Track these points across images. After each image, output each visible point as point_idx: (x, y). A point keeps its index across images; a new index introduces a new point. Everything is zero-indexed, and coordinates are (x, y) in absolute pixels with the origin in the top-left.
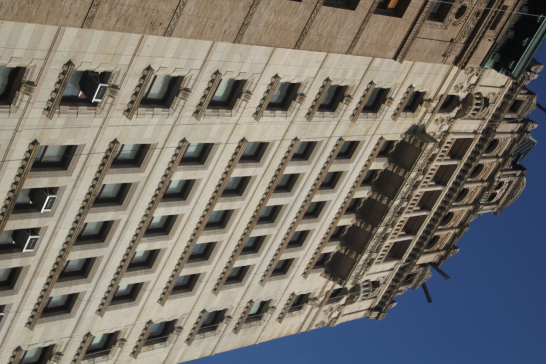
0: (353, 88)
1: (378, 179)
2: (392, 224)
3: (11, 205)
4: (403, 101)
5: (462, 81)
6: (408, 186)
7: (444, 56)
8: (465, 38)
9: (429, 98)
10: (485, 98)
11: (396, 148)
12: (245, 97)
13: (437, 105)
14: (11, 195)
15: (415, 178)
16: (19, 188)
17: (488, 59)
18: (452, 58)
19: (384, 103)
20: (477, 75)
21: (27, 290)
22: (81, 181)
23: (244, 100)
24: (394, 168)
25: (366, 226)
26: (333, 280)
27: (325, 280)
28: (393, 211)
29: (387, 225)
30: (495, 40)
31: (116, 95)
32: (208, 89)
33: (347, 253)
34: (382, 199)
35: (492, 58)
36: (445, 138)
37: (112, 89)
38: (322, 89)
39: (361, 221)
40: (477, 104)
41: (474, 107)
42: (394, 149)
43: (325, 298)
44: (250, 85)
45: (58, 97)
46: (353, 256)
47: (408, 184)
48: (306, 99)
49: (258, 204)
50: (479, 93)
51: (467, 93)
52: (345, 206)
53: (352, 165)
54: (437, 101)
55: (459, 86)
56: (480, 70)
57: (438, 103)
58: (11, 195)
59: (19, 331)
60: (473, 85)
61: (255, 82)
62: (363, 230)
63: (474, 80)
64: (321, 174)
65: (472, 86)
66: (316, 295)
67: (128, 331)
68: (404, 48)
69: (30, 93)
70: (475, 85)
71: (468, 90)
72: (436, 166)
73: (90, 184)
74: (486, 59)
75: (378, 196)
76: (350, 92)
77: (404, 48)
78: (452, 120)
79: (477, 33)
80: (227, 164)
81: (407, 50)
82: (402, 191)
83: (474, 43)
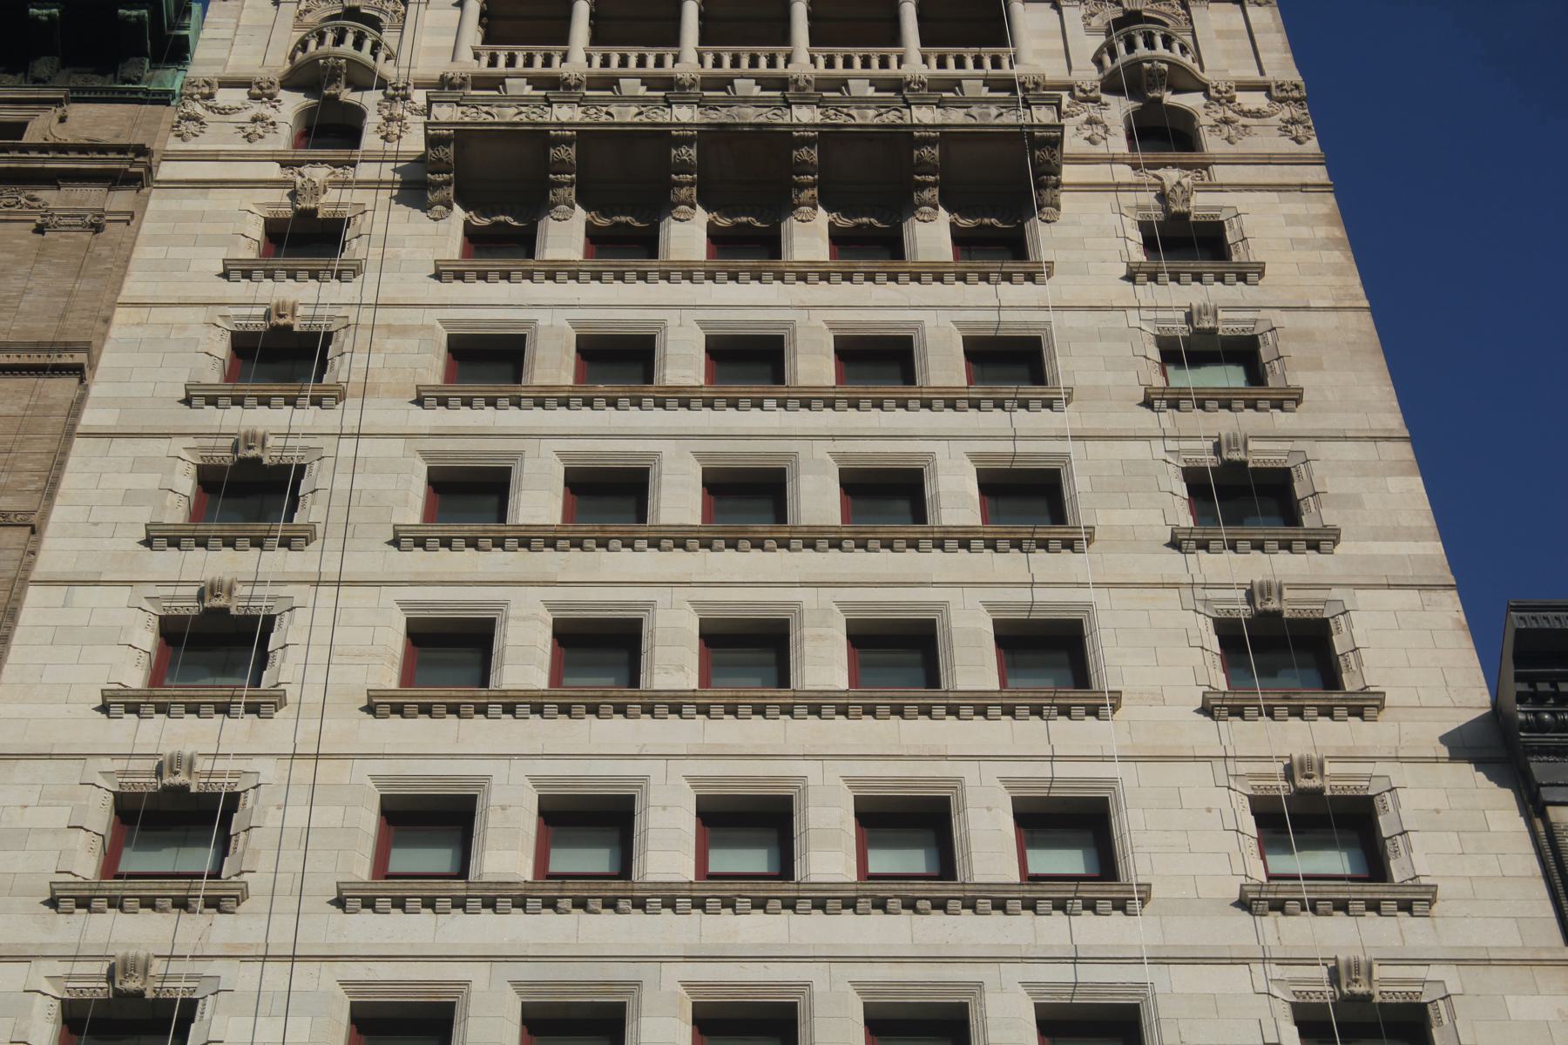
0: (204, 449)
1: (626, 215)
2: (839, 90)
4: (281, 274)
5: (231, 129)
6: (613, 109)
7: (97, 228)
8: (37, 194)
9: (287, 200)
10: (1108, 33)
11: (495, 214)
12: (176, 773)
13: (323, 162)
15: (758, 102)
17: (147, 92)
18: (120, 200)
19: (289, 327)
20: (210, 96)
23: (190, 772)
24: (561, 185)
25: (803, 167)
26: (1056, 171)
27: (1065, 198)
28: (724, 110)
29: (965, 104)
30: (58, 102)
32: (149, 903)
33: (931, 178)
34: (684, 167)
35: (139, 80)
36: (457, 81)
38: (184, 542)
39: (794, 192)
40: (358, 45)
41: (347, 47)
42: (502, 218)
43: (1165, 166)
44: (134, 773)
46: (931, 153)
47: (608, 113)
48: (209, 575)
50: (1098, 61)
51: (283, 95)
52: (723, 269)
53: (543, 318)
54: (306, 170)
55: (1087, 133)
56: (191, 96)
57: (314, 162)
60: (1269, 96)
62: (702, 167)
63: (1256, 100)
64: (468, 402)
65: (1078, 93)
66: (1148, 198)
67: (1243, 768)
68: (35, 359)
70: (1265, 88)
71: (271, 97)
72: (813, 60)
74: (140, 95)
75: (681, 185)
76: (222, 449)
77: (24, 360)
78: (1213, 93)
79: (8, 168)
80: (479, 720)
81: (38, 347)
82: (877, 121)
83: (45, 160)
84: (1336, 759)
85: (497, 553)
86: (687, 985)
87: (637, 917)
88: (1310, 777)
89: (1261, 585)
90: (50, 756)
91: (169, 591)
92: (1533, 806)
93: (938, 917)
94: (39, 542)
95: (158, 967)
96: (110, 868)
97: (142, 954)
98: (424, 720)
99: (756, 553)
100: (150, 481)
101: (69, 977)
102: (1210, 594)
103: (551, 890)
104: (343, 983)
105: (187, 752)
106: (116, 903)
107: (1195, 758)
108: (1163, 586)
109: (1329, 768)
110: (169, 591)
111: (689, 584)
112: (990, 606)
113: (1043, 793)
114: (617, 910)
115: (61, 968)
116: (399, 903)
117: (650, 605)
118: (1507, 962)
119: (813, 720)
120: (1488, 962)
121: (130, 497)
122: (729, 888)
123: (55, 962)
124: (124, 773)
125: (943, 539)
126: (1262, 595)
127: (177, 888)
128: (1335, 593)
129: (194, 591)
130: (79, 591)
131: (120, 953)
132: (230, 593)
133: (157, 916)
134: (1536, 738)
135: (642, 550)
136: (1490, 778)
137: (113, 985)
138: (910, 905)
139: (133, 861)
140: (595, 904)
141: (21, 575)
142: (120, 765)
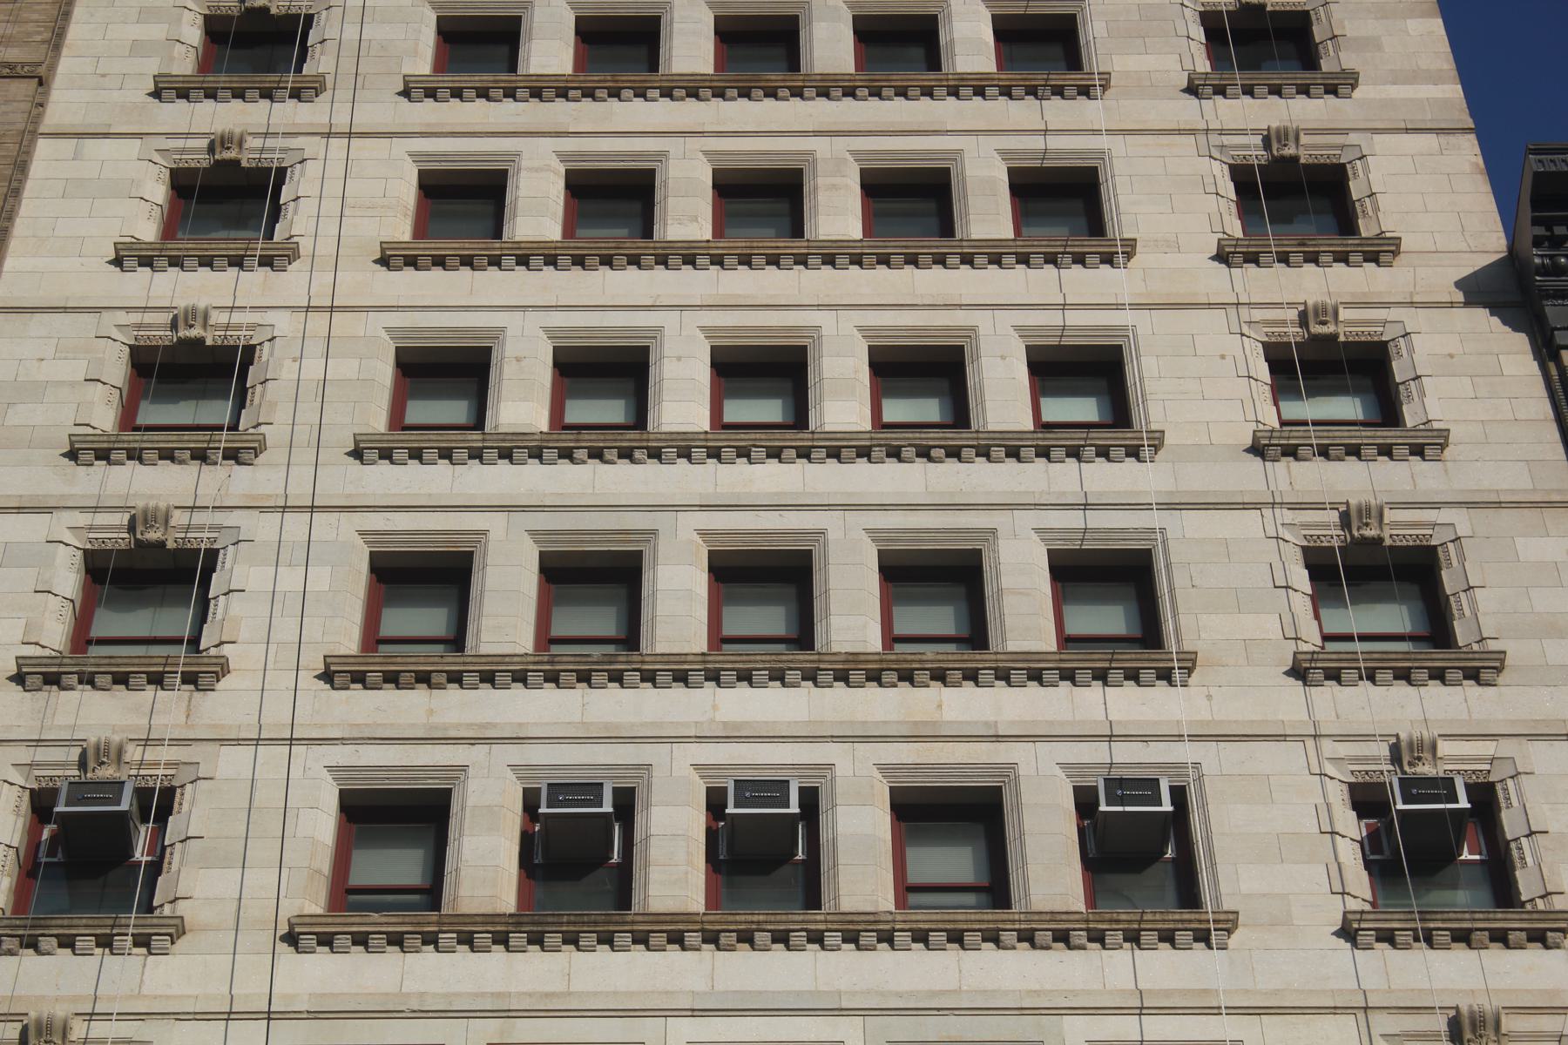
3: (561, 924)
12: (191, 326)
14: (517, 939)
16: (483, 923)
21: (998, 738)
22: (494, 726)
23: (205, 325)
31: (107, 744)
32: (168, 455)
37: (91, 764)
38: (192, 94)
44: (149, 326)
45: (86, 926)
49: (691, 102)
58: (517, 939)
59: (1209, 697)
61: (123, 318)
67: (1258, 315)
69: (58, 1025)
73: (518, 690)
80: (493, 272)
84: (1349, 305)
85: (509, 104)
86: (703, 533)
87: (652, 467)
88: (1324, 323)
89: (1278, 130)
90: (65, 310)
91: (180, 143)
92: (1546, 350)
93: (952, 465)
94: (47, 94)
95: (179, 518)
96: (128, 420)
97: (162, 505)
98: (437, 273)
99: (769, 103)
100: (157, 32)
101: (91, 528)
102: (1226, 140)
103: (567, 440)
104: (362, 533)
105: (202, 305)
106: (135, 455)
107: (1210, 306)
108: (1179, 132)
109: (1344, 314)
110: (180, 143)
111: (702, 134)
112: (1005, 154)
113: (1054, 341)
114: (633, 461)
115: (83, 519)
116: (416, 454)
117: (662, 156)
118: (1517, 505)
119: (827, 271)
120: (1498, 505)
121: (138, 48)
122: (744, 438)
123: (76, 513)
124: (139, 326)
125: (957, 87)
126: (1279, 141)
127: (197, 440)
128: (1353, 138)
129: (204, 143)
130: (90, 143)
131: (140, 504)
132: (240, 145)
133: (175, 468)
134: (1552, 282)
135: (654, 100)
136: (1505, 322)
137: (135, 535)
138: (924, 453)
139: (151, 413)
140: (611, 454)
141: (30, 127)
142: (135, 318)
